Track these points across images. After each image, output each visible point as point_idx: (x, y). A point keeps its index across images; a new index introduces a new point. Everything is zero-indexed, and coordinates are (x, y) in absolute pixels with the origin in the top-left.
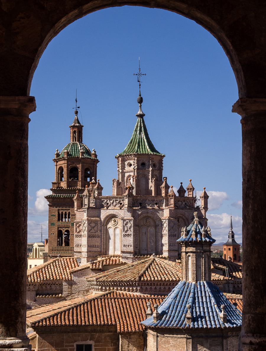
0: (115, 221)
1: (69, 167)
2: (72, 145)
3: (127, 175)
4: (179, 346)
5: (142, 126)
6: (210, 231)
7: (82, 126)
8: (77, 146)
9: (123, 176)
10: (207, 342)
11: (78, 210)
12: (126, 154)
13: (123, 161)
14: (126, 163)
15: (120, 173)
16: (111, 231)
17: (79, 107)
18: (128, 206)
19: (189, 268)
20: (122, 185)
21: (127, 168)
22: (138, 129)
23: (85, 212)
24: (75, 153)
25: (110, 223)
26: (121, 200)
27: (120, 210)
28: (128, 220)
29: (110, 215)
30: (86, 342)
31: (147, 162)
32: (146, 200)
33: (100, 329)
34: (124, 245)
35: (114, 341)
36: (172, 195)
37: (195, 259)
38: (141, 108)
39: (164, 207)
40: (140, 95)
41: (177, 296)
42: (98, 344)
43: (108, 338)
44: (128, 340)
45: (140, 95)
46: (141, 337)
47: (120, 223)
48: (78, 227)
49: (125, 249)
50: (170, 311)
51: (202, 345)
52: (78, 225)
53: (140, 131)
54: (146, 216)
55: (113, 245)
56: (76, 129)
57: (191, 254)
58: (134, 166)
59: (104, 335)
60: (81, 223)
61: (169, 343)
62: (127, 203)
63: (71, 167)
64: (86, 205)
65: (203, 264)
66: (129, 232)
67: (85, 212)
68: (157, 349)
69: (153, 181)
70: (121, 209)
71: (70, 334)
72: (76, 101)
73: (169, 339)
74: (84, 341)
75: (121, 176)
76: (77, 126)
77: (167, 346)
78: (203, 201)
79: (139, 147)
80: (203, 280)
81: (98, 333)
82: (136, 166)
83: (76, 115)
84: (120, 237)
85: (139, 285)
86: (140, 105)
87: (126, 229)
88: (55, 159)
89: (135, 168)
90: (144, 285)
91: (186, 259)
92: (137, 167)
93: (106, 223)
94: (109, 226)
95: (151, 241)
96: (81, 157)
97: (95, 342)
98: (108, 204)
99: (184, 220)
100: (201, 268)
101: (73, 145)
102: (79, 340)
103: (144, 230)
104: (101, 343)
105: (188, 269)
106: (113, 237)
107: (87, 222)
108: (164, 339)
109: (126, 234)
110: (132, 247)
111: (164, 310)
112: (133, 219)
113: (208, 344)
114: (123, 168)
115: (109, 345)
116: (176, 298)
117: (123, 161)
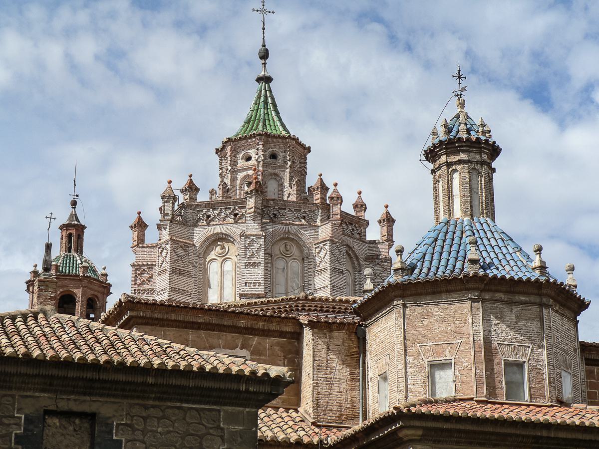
0: (223, 248)
1: (59, 292)
2: (64, 258)
3: (240, 175)
4: (454, 318)
5: (268, 95)
6: (490, 132)
7: (83, 227)
8: (74, 259)
9: (233, 180)
10: (511, 311)
11: (140, 245)
12: (243, 136)
13: (235, 151)
14: (240, 156)
15: (228, 172)
16: (214, 270)
17: (77, 196)
18: (254, 212)
19: (454, 194)
20: (231, 194)
21: (241, 163)
22: (262, 99)
23: (165, 229)
24: (71, 269)
25: (213, 252)
26: (236, 208)
27: (235, 225)
28: (253, 235)
29: (213, 235)
30: (234, 351)
31: (280, 152)
32: (285, 209)
33: (264, 325)
34: (246, 283)
35: (290, 356)
36: (338, 198)
37: (467, 174)
38: (265, 67)
39: (319, 224)
40: (264, 46)
41: (436, 240)
42: (258, 357)
43: (278, 348)
44: (326, 340)
45: (264, 46)
46: (353, 337)
47: (233, 251)
48: (139, 275)
49: (247, 290)
50: (426, 264)
51: (501, 318)
52: (138, 272)
53: (266, 102)
54: (283, 239)
55: (219, 292)
56: (73, 232)
57: (459, 167)
58: (257, 156)
59: (268, 342)
60: (145, 268)
61: (432, 316)
62: (254, 205)
63: (61, 292)
64: (167, 214)
65: (483, 187)
66: (256, 259)
67: (165, 229)
68: (404, 330)
69: (294, 183)
70: (236, 222)
71: (202, 331)
72: (75, 185)
73: (431, 309)
74: (229, 349)
75: (231, 177)
76: (75, 225)
77: (426, 321)
78: (386, 227)
79: (264, 125)
80: (485, 215)
81: (258, 335)
82: (262, 156)
83: (73, 208)
84: (234, 277)
85: (304, 309)
86: (263, 62)
87: (249, 254)
88: (30, 281)
89: (261, 159)
90: (315, 310)
91: (448, 177)
92: (263, 158)
93: (205, 252)
94: (212, 255)
95: (294, 285)
96: (81, 274)
97: (252, 354)
98: (209, 216)
99: (351, 258)
100: (478, 193)
101: (67, 257)
102: (220, 345)
103: (280, 264)
104: (263, 358)
105: (452, 195)
106: (220, 278)
107: (168, 247)
108: (418, 310)
109: (250, 263)
110: (262, 287)
111: (415, 261)
112: (264, 234)
113: (514, 315)
114: (234, 163)
115: (278, 361)
116: (434, 243)
117: (235, 151)
